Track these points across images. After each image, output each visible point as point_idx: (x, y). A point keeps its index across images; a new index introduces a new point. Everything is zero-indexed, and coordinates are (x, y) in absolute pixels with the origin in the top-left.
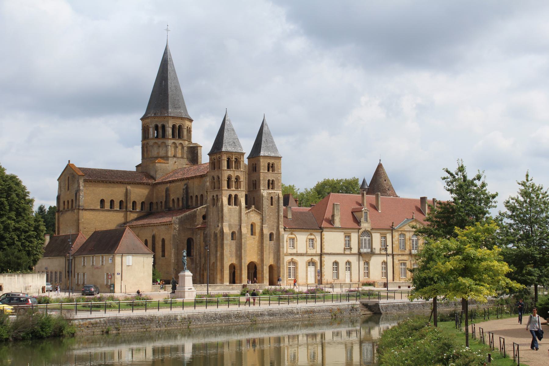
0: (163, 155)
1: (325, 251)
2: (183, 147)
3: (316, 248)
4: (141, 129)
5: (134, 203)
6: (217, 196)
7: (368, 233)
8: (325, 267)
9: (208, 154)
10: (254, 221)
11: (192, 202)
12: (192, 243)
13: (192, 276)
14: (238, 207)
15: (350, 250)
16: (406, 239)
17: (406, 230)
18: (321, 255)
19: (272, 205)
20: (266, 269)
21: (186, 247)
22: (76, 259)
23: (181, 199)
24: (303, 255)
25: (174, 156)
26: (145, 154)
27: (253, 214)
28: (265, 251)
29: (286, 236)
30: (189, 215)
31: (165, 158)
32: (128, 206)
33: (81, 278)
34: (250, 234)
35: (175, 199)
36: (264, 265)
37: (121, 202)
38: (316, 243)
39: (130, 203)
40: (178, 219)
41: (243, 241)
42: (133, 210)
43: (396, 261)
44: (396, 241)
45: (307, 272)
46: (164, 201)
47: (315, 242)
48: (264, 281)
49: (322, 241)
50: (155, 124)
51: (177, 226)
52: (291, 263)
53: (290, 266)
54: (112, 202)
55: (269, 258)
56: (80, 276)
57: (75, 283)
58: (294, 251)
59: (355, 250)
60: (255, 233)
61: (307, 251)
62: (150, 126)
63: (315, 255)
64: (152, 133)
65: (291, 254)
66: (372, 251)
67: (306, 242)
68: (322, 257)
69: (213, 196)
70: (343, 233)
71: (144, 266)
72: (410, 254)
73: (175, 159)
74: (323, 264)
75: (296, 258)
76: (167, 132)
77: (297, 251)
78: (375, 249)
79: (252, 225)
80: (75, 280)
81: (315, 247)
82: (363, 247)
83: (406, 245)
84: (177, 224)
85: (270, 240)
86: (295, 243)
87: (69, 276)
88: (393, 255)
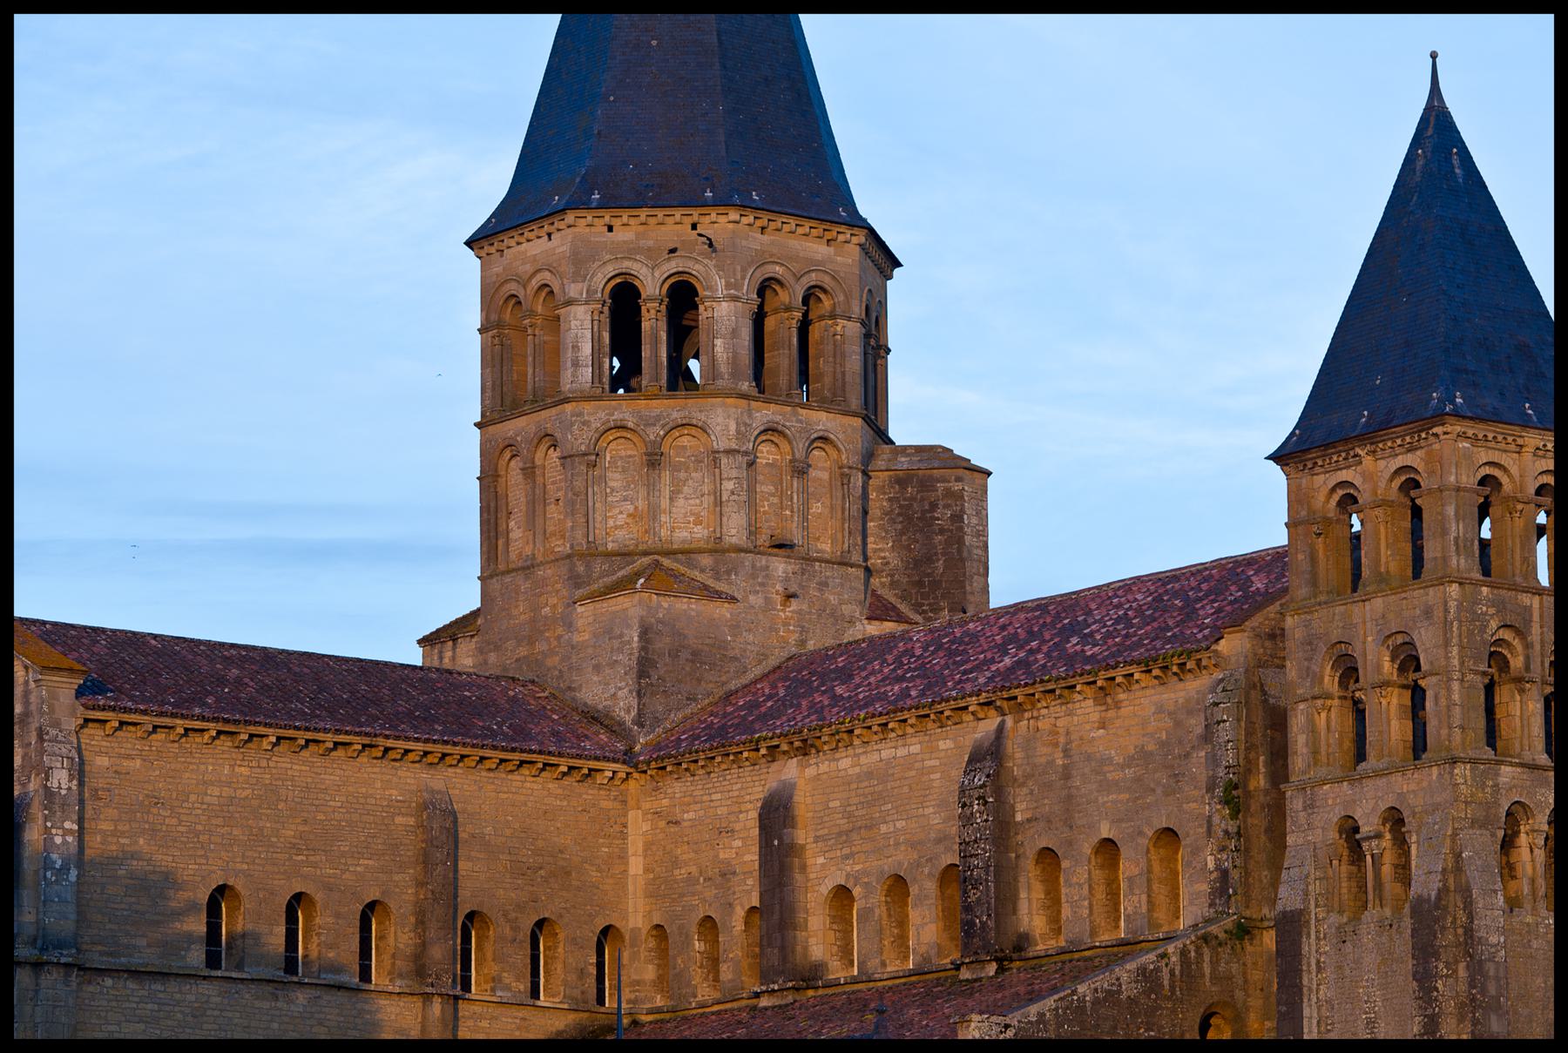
0: (681, 535)
4: (476, 320)
6: (1395, 819)
9: (1278, 457)
11: (1053, 901)
23: (925, 888)
26: (516, 533)
30: (1096, 1002)
35: (856, 892)
46: (740, 912)
50: (610, 270)
62: (574, 290)
64: (586, 349)
69: (1350, 829)
73: (780, 566)
76: (718, 342)
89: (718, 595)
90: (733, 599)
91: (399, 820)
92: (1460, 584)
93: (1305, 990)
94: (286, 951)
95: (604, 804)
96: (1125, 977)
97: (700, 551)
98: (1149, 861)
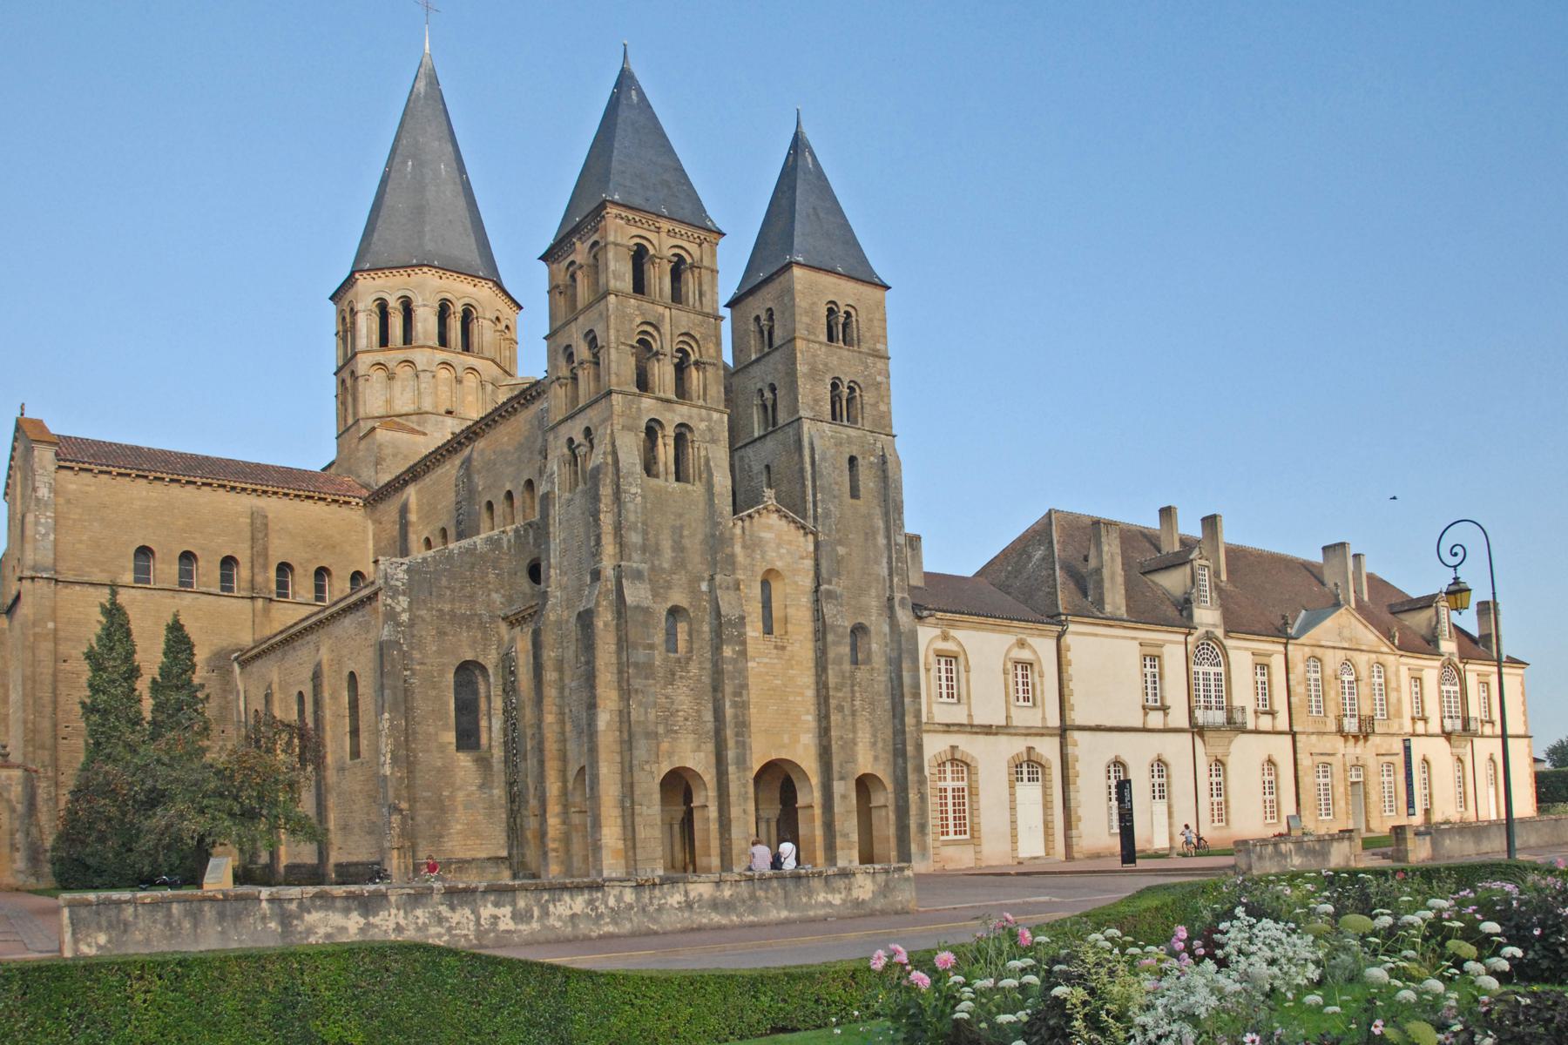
1: (1077, 717)
2: (482, 384)
3: (1043, 704)
5: (284, 568)
7: (1211, 648)
8: (1079, 781)
10: (779, 565)
12: (482, 689)
14: (697, 489)
15: (1161, 713)
16: (1327, 678)
17: (1323, 643)
18: (1064, 731)
19: (855, 493)
20: (844, 797)
21: (452, 706)
24: (996, 734)
25: (449, 413)
27: (770, 528)
28: (840, 708)
29: (927, 636)
30: (460, 554)
31: (414, 418)
32: (259, 579)
34: (760, 625)
36: (835, 775)
37: (229, 562)
38: (1042, 684)
39: (265, 567)
40: (408, 571)
41: (728, 651)
42: (279, 595)
43: (1305, 761)
44: (1299, 683)
45: (1013, 809)
47: (1036, 675)
48: (839, 853)
49: (1065, 676)
51: (404, 601)
52: (948, 767)
53: (942, 784)
54: (187, 557)
58: (958, 715)
59: (1179, 717)
60: (786, 620)
61: (1008, 717)
63: (1042, 732)
65: (948, 728)
66: (1230, 721)
67: (1005, 672)
68: (1069, 740)
70: (1136, 643)
72: (1341, 731)
73: (449, 421)
74: (1071, 772)
77: (970, 716)
78: (1243, 709)
79: (765, 584)
81: (1039, 702)
82: (1202, 703)
83: (1327, 698)
84: (404, 594)
85: (855, 662)
86: (963, 675)
88: (1294, 735)
89: (418, 432)
90: (425, 434)
91: (241, 520)
92: (616, 296)
93: (552, 535)
94: (180, 577)
95: (354, 517)
96: (479, 542)
97: (411, 415)
98: (523, 497)
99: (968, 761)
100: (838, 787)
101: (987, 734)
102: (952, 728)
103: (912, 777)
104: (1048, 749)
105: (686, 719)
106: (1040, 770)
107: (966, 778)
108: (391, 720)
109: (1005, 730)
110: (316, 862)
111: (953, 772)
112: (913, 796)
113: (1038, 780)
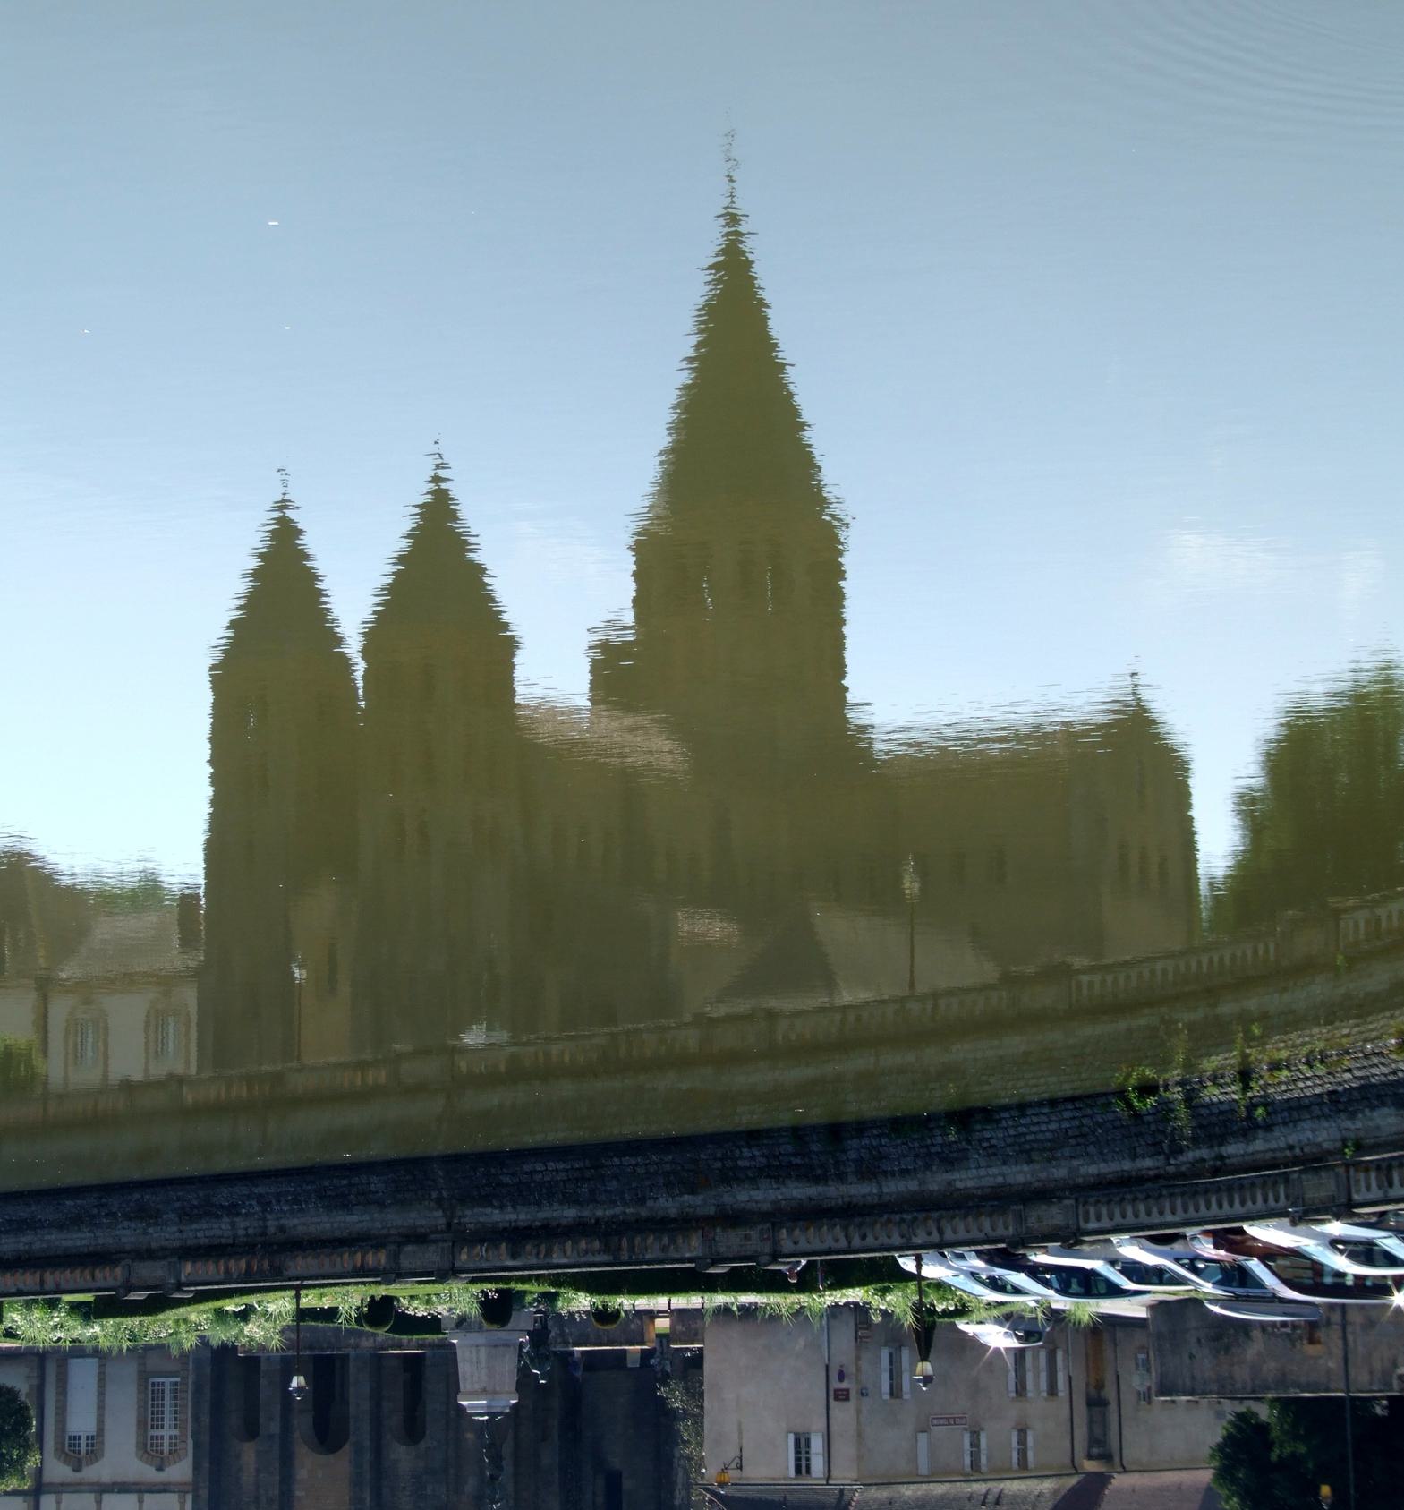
13: (458, 1391)
22: (1067, 1460)
24: (114, 1484)
33: (1037, 1376)
55: (258, 1471)
56: (1044, 1385)
57: (1066, 1352)
65: (164, 1488)
71: (740, 1433)
75: (149, 1474)
77: (141, 1501)
80: (1067, 1367)
87: (1100, 1386)
99: (146, 1455)
100: (275, 1428)
101: (124, 1484)
102: (162, 1488)
103: (206, 1438)
104: (58, 1471)
105: (404, 1488)
106: (67, 1449)
107: (149, 1438)
108: (673, 1497)
109: (101, 1489)
110: (629, 1365)
111: (162, 1445)
112: (206, 1420)
113: (70, 1437)
